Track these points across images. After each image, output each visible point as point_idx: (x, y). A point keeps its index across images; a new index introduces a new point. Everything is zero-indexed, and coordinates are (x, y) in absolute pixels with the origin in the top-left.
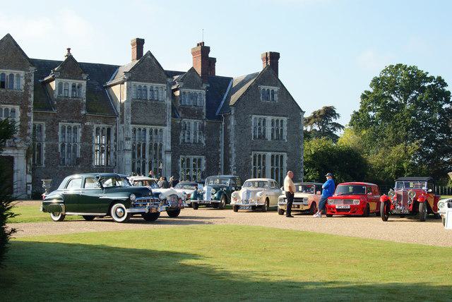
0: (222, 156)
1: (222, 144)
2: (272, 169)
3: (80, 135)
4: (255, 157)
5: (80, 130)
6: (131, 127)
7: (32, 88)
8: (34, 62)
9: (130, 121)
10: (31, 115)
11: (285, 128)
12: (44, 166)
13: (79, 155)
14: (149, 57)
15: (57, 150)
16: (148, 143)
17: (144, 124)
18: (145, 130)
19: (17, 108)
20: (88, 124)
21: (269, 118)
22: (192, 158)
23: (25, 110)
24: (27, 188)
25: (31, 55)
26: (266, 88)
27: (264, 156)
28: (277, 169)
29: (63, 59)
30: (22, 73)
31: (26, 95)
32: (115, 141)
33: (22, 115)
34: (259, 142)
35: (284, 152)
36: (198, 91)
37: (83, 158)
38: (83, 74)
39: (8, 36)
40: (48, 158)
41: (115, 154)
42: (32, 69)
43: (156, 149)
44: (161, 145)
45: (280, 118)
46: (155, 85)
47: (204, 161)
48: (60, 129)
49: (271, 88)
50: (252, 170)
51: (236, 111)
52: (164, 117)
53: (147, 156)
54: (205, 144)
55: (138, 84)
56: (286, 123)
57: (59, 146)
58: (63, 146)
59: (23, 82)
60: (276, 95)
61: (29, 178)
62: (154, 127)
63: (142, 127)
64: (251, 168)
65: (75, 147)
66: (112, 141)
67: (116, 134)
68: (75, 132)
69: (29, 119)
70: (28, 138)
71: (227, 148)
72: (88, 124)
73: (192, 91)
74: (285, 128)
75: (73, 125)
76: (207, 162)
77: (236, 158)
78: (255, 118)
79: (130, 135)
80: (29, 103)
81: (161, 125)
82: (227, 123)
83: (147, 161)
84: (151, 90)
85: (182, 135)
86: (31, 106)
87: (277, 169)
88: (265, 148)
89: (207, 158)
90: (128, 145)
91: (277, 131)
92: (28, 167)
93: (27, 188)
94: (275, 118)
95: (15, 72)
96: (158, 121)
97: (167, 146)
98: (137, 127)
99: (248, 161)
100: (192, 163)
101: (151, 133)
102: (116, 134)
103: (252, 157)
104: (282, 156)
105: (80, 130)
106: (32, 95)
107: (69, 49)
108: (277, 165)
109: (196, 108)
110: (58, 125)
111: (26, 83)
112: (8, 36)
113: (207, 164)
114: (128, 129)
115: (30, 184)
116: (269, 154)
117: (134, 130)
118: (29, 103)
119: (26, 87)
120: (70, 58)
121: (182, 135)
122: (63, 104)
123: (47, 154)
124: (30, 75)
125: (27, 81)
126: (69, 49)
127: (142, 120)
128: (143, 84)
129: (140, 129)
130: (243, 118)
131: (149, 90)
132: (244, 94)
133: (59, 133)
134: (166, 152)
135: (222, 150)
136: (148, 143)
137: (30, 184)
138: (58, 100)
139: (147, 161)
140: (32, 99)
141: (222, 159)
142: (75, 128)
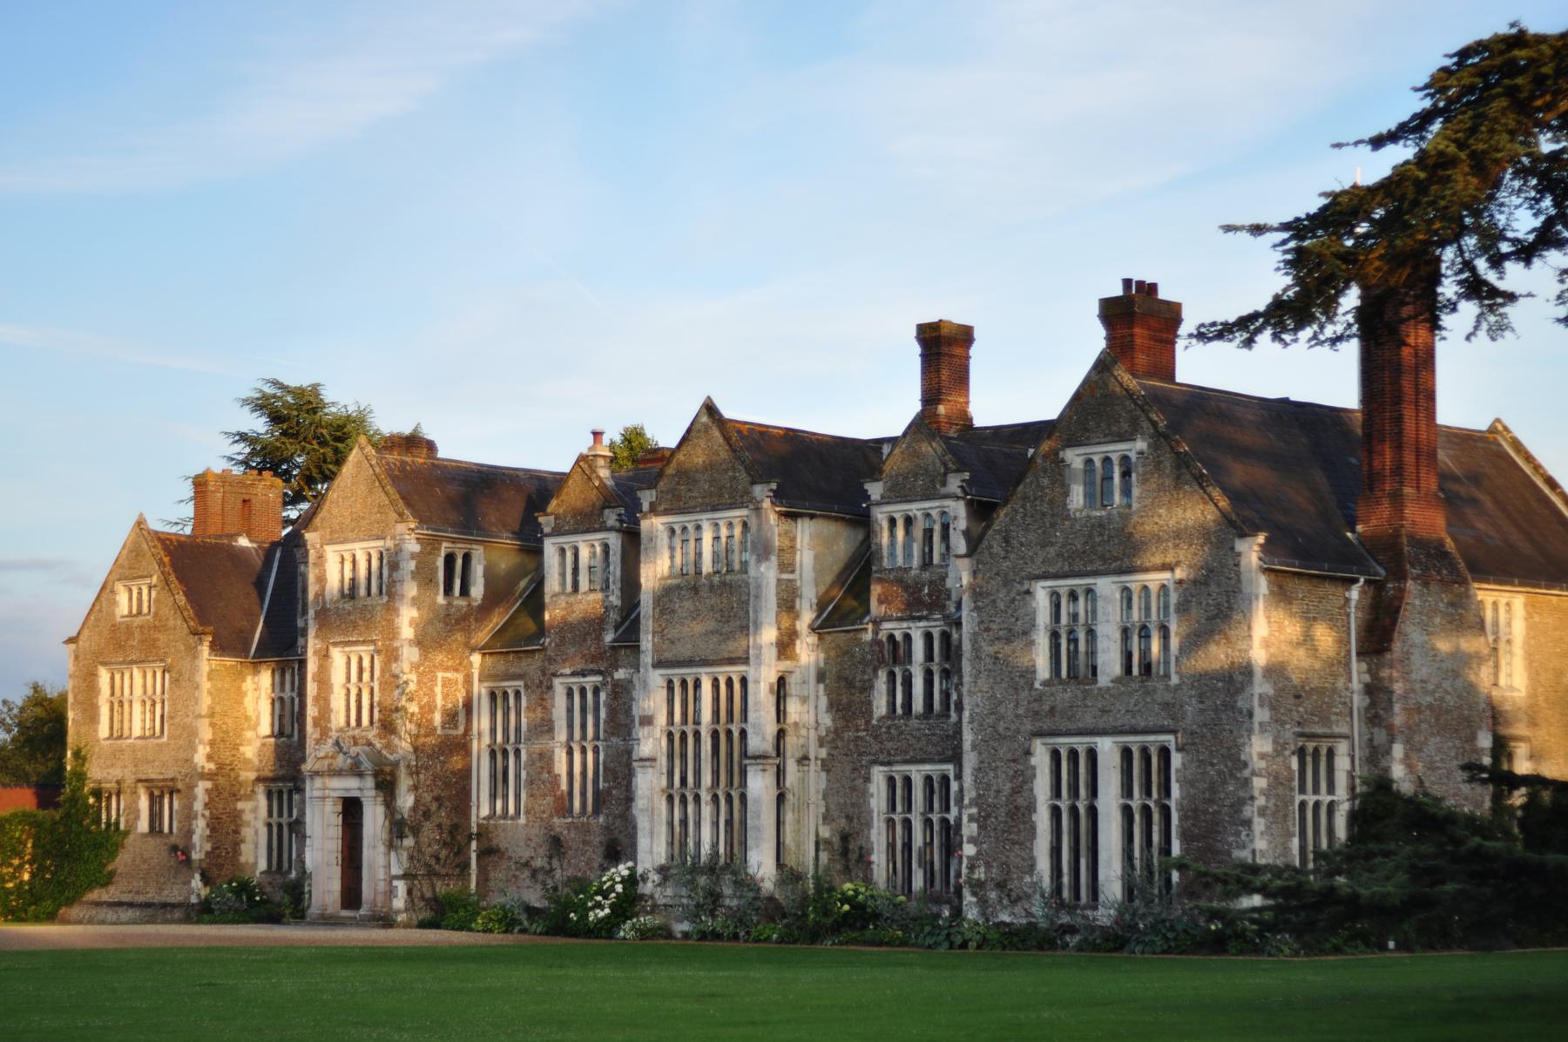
5: (603, 696)
6: (657, 678)
14: (704, 419)
17: (690, 663)
20: (620, 674)
22: (917, 773)
26: (1097, 452)
27: (1092, 755)
33: (383, 671)
34: (1064, 696)
35: (1174, 732)
38: (607, 511)
44: (743, 733)
49: (1116, 450)
53: (707, 779)
64: (1031, 808)
72: (620, 674)
73: (915, 509)
77: (978, 770)
78: (1055, 598)
81: (732, 661)
88: (1088, 720)
93: (391, 893)
98: (677, 673)
99: (1023, 779)
104: (1165, 753)
108: (1074, 792)
109: (926, 575)
110: (550, 687)
115: (397, 877)
116: (1107, 748)
123: (531, 782)
127: (685, 651)
137: (397, 877)
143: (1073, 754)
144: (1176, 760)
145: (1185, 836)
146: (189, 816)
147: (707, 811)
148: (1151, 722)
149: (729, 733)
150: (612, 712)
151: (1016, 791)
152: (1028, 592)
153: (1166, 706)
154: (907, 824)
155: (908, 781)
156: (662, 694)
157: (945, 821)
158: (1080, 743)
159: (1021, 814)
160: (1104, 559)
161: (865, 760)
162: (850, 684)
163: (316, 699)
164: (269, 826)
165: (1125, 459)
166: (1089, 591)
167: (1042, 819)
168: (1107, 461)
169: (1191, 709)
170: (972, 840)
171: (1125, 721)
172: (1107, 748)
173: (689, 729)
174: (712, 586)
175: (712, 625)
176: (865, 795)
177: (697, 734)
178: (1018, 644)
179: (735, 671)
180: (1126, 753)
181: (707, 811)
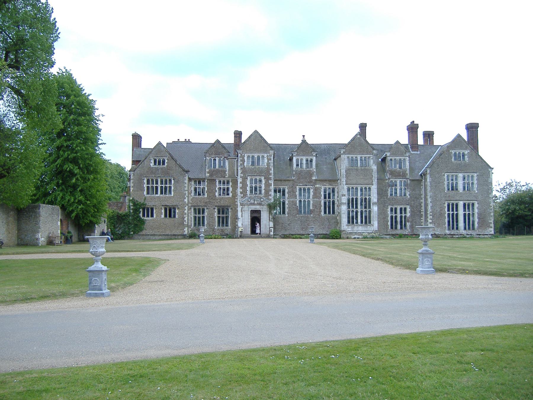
0: (423, 205)
1: (423, 196)
2: (465, 215)
3: (312, 194)
4: (448, 205)
5: (312, 190)
7: (272, 164)
8: (271, 147)
9: (344, 183)
10: (272, 182)
11: (475, 182)
12: (287, 215)
13: (311, 208)
15: (295, 205)
16: (359, 197)
18: (357, 189)
19: (263, 178)
20: (317, 186)
21: (460, 175)
23: (267, 179)
24: (270, 231)
25: (270, 141)
28: (469, 214)
29: (299, 142)
30: (265, 155)
31: (268, 169)
32: (338, 197)
36: (402, 158)
37: (314, 210)
39: (256, 132)
40: (289, 210)
41: (338, 206)
42: (272, 152)
43: (366, 201)
44: (370, 199)
45: (470, 174)
46: (363, 156)
47: (408, 210)
48: (298, 190)
50: (446, 215)
51: (430, 171)
52: (371, 178)
54: (409, 197)
55: (350, 156)
56: (476, 178)
57: (298, 202)
58: (300, 201)
59: (266, 161)
60: (466, 157)
61: (272, 225)
62: (364, 186)
63: (354, 186)
65: (309, 202)
66: (336, 197)
67: (338, 192)
68: (309, 193)
69: (271, 185)
70: (270, 197)
71: (426, 200)
72: (317, 186)
73: (398, 158)
74: (475, 182)
75: (306, 187)
76: (411, 210)
78: (448, 176)
79: (345, 192)
80: (270, 174)
82: (426, 180)
83: (359, 210)
84: (361, 160)
85: (389, 190)
86: (272, 176)
87: (469, 214)
88: (458, 198)
89: (411, 207)
90: (344, 200)
91: (468, 184)
92: (271, 217)
94: (466, 175)
95: (261, 155)
96: (366, 182)
97: (374, 198)
98: (351, 186)
99: (442, 209)
100: (398, 211)
101: (361, 190)
102: (338, 192)
103: (446, 205)
104: (473, 204)
105: (312, 190)
106: (272, 169)
107: (304, 136)
109: (401, 170)
111: (268, 161)
112: (256, 132)
113: (411, 212)
114: (343, 188)
116: (461, 204)
117: (348, 190)
118: (270, 174)
119: (268, 164)
120: (304, 141)
121: (389, 190)
122: (300, 174)
123: (289, 208)
124: (271, 156)
125: (269, 160)
126: (304, 136)
127: (354, 182)
128: (354, 156)
129: (353, 188)
130: (437, 176)
131: (359, 159)
132: (229, 164)
133: (297, 193)
134: (374, 203)
135: (423, 201)
136: (359, 197)
138: (296, 171)
139: (359, 210)
140: (272, 172)
141: (423, 208)
142: (309, 189)
143: (453, 204)
144: (476, 205)
145: (479, 218)
146: (183, 213)
147: (359, 214)
148: (471, 199)
149: (366, 199)
150: (315, 194)
151: (441, 210)
152: (444, 175)
153: (474, 196)
154: (396, 217)
155: (396, 209)
156: (346, 190)
157: (405, 216)
158: (455, 202)
159: (442, 215)
160: (460, 170)
161: (386, 204)
162: (382, 190)
163: (241, 188)
164: (195, 217)
165: (463, 153)
166: (456, 176)
167: (476, 215)
168: (459, 153)
169: (480, 197)
170: (430, 219)
171: (466, 198)
172: (461, 204)
173: (355, 197)
174: (362, 170)
175: (362, 177)
176: (387, 211)
177: (357, 199)
178: (441, 184)
179: (367, 187)
180: (464, 205)
181: (359, 214)
